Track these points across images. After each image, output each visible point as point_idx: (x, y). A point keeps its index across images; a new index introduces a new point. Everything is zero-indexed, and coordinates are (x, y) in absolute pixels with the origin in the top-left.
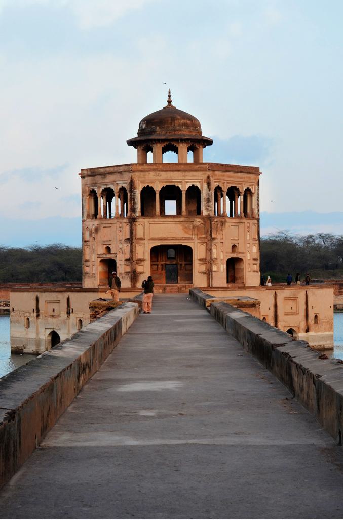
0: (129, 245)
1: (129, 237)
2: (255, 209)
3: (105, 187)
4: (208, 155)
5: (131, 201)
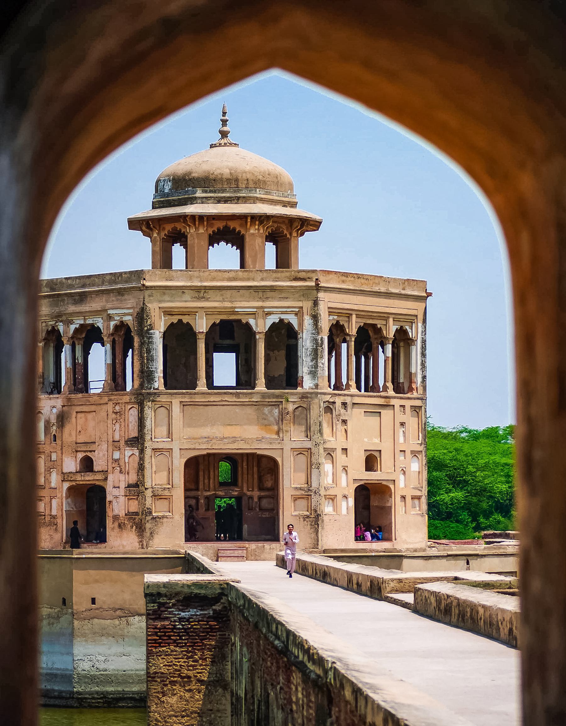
0: (137, 452)
1: (136, 435)
2: (416, 374)
3: (82, 322)
4: (309, 252)
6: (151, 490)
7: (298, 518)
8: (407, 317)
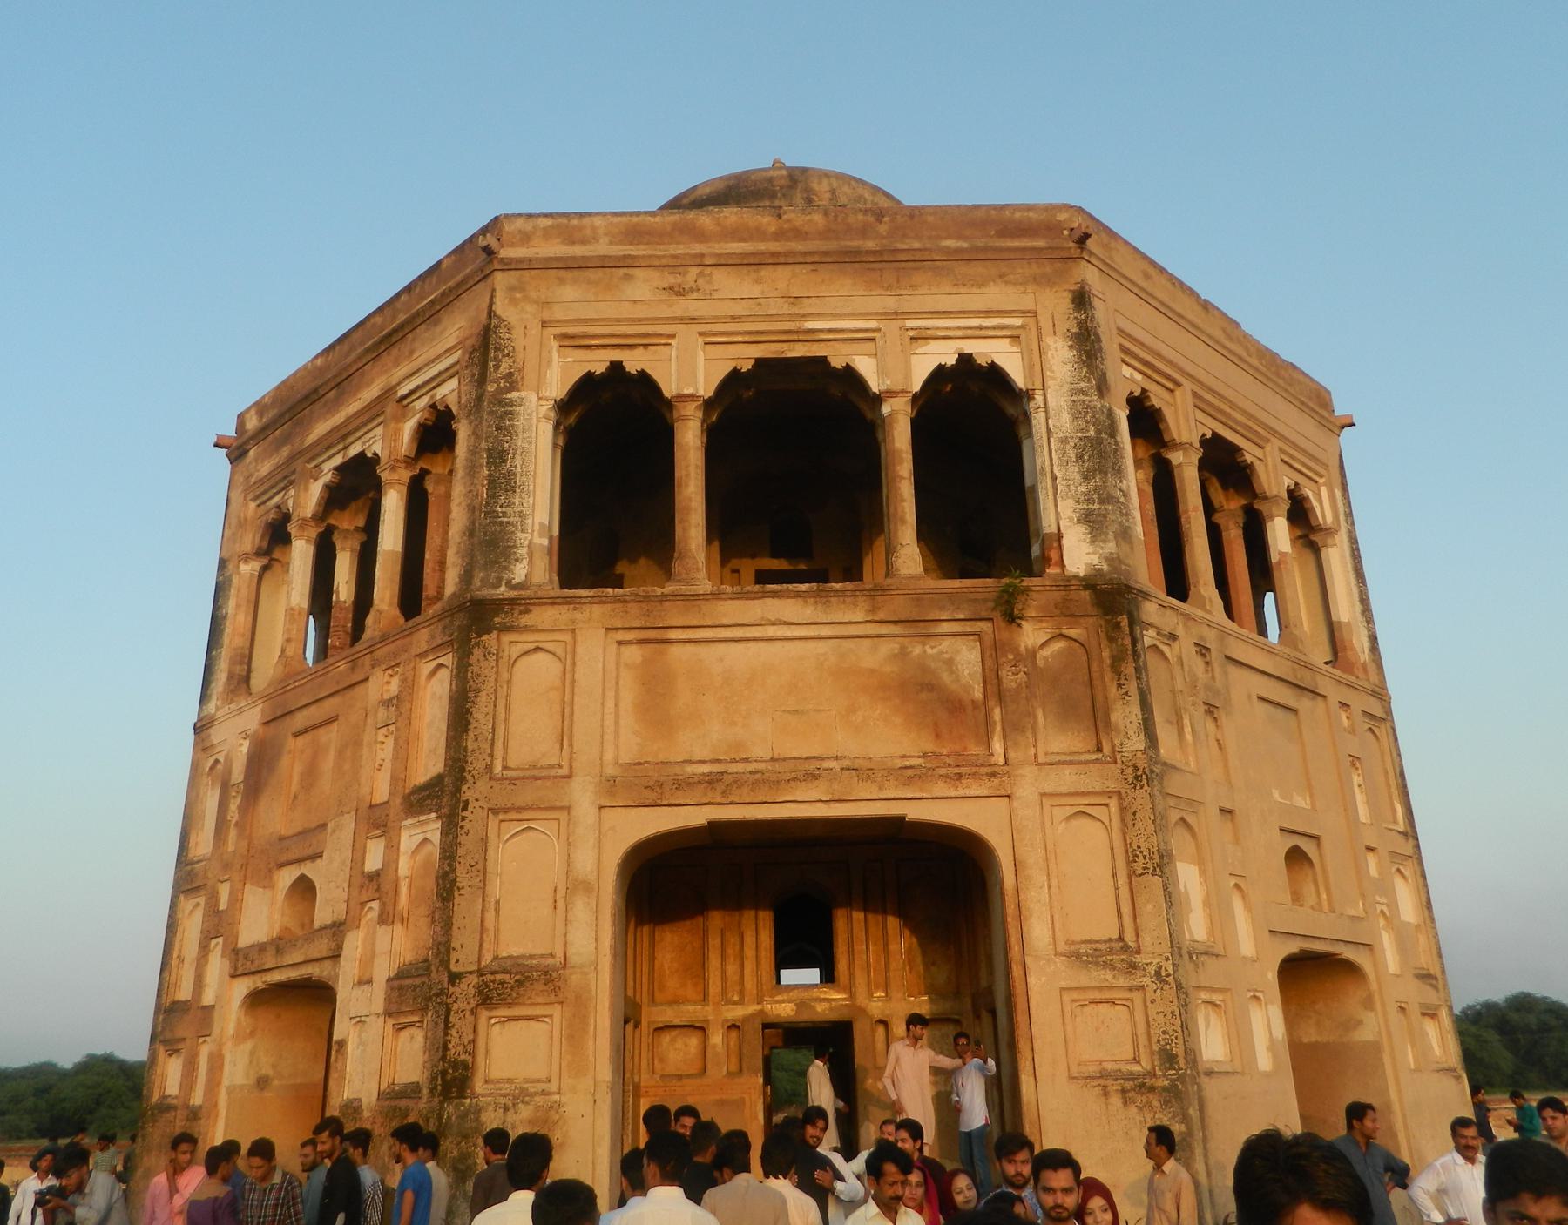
3: (338, 460)
5: (472, 470)
6: (474, 979)
7: (1098, 1090)
8: (1306, 461)
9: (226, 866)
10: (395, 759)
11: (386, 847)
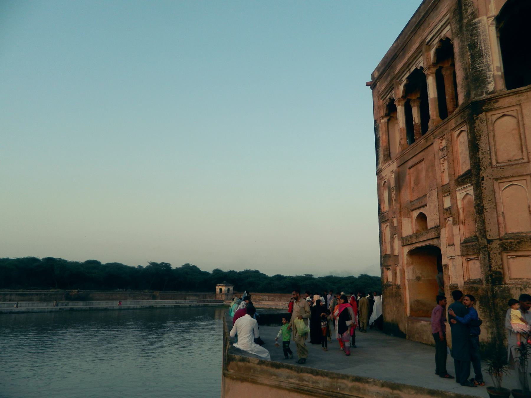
0: (471, 190)
3: (407, 75)
6: (498, 242)
9: (394, 213)
10: (449, 168)
11: (451, 199)
